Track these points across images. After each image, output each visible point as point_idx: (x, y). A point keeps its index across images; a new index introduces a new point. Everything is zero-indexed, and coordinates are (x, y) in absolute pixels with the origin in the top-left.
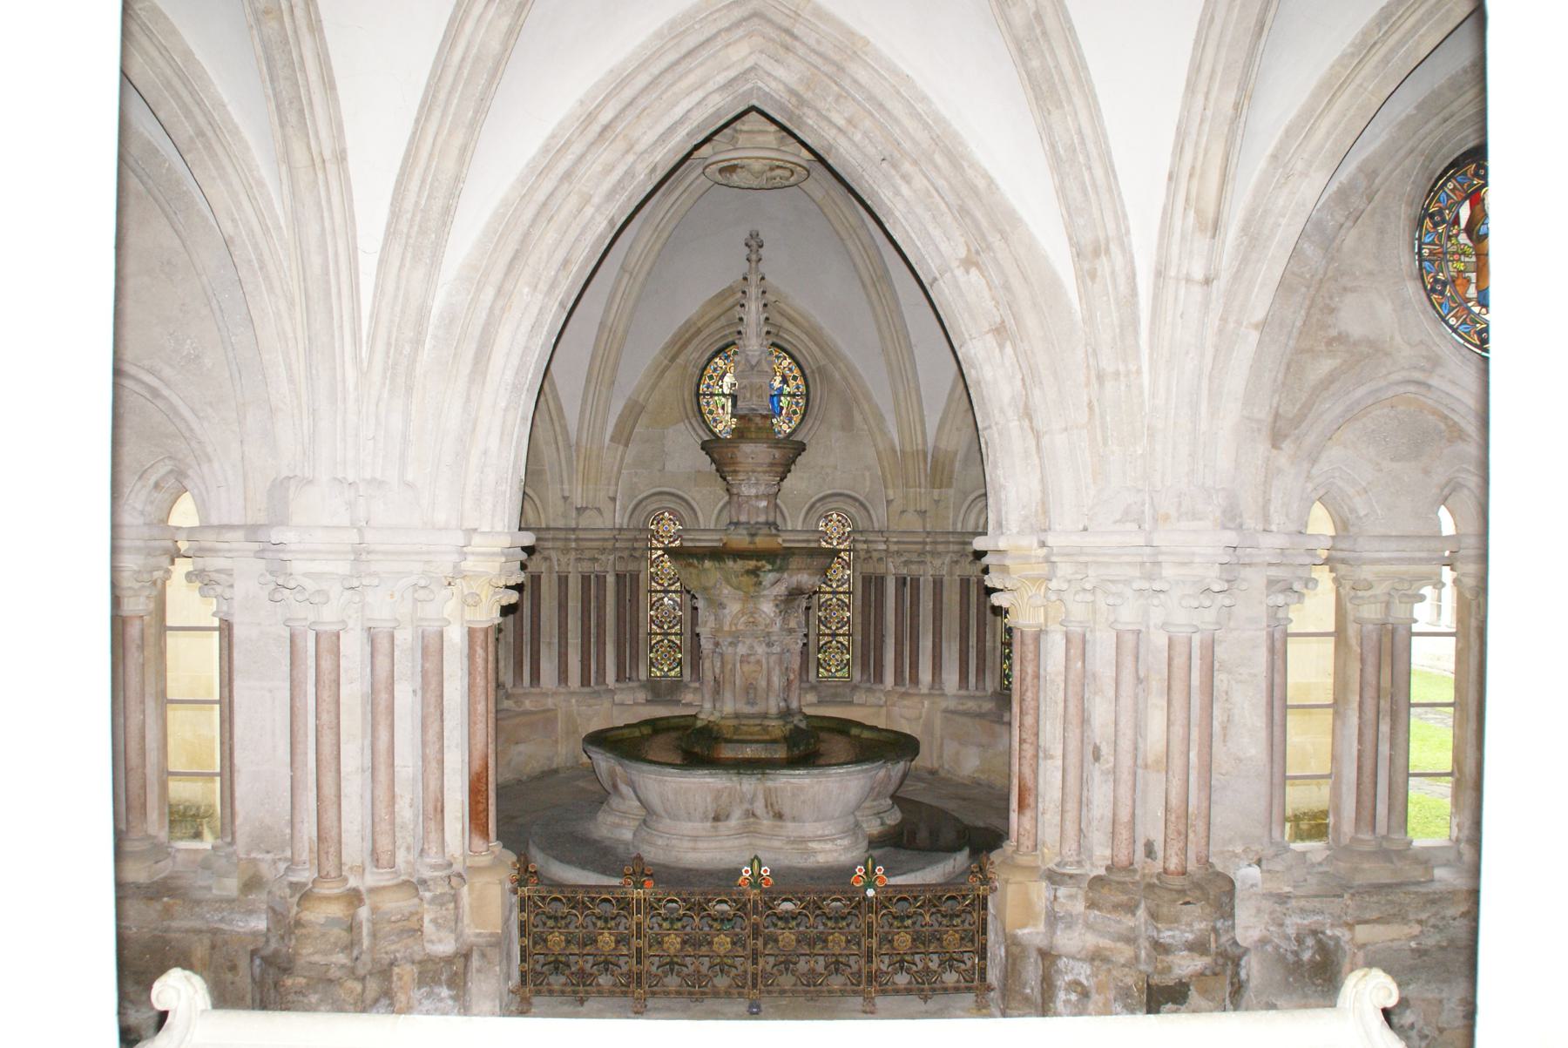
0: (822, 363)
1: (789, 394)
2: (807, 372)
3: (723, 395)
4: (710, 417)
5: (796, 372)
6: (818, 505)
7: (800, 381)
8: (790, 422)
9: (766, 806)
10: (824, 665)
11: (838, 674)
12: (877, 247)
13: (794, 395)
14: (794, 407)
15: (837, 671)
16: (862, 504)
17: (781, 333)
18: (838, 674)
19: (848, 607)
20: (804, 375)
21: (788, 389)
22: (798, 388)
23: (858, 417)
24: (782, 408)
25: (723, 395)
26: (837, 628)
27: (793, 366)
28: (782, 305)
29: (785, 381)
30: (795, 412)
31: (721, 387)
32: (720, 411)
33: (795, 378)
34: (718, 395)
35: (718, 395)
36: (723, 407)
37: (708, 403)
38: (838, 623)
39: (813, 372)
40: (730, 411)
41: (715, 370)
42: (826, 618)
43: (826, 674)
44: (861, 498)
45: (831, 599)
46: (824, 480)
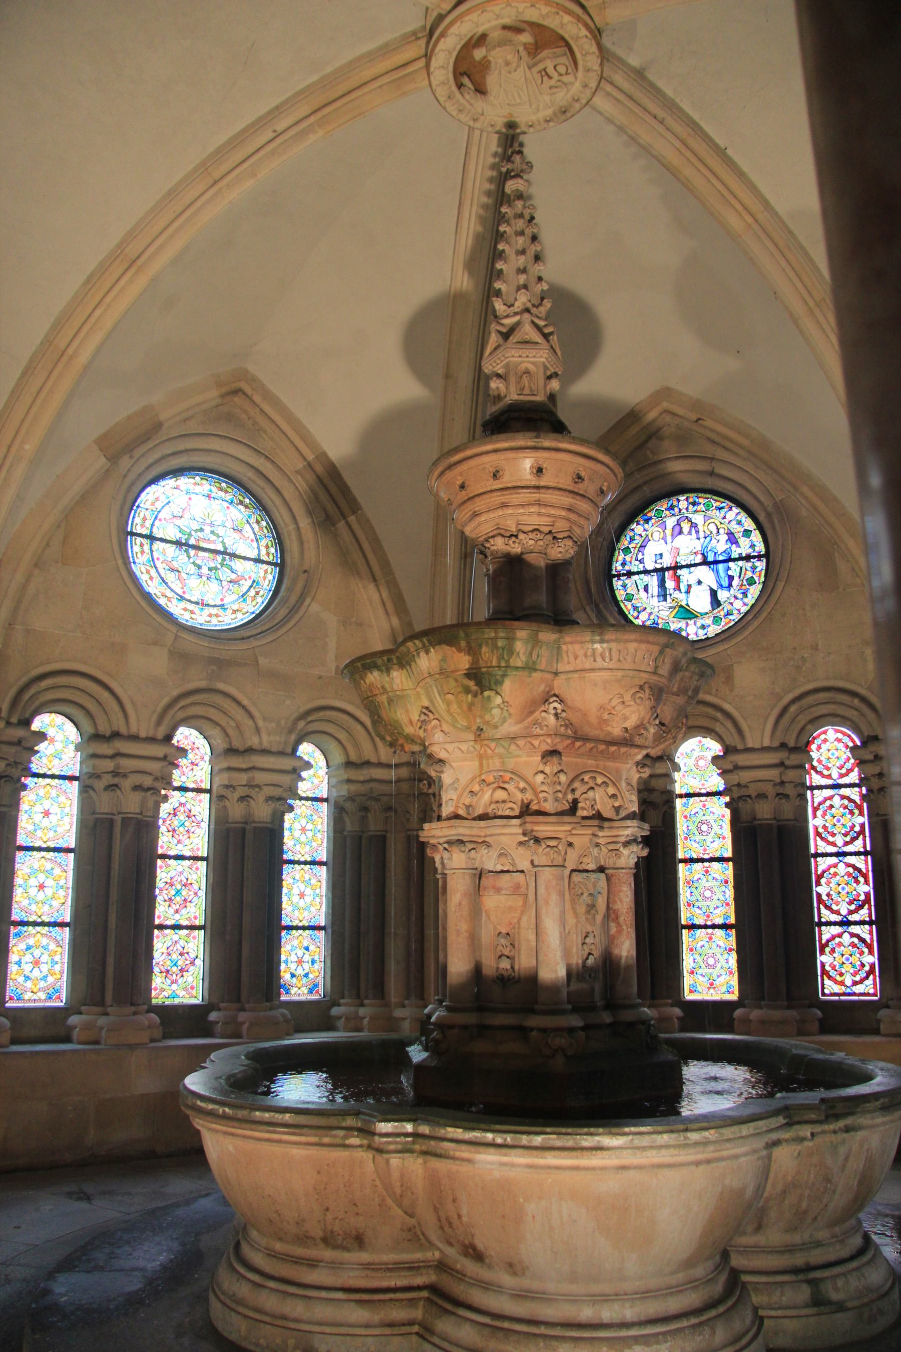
0: (779, 497)
1: (741, 558)
2: (762, 517)
3: (646, 572)
4: (629, 605)
5: (749, 524)
6: (793, 708)
7: (756, 537)
8: (745, 594)
9: (442, 1228)
10: (832, 973)
11: (859, 989)
12: (802, 248)
13: (748, 558)
14: (749, 574)
15: (855, 983)
16: (863, 699)
17: (716, 471)
18: (859, 989)
19: (865, 876)
20: (760, 527)
21: (739, 551)
22: (752, 546)
23: (842, 567)
24: (731, 578)
25: (646, 572)
26: (851, 912)
27: (743, 516)
28: (709, 423)
29: (732, 539)
30: (751, 582)
31: (641, 561)
32: (643, 594)
33: (747, 533)
34: (638, 573)
35: (638, 573)
36: (646, 589)
37: (624, 586)
38: (850, 903)
39: (769, 515)
40: (656, 593)
41: (632, 539)
42: (828, 895)
43: (837, 989)
44: (863, 691)
45: (835, 866)
46: (798, 668)
